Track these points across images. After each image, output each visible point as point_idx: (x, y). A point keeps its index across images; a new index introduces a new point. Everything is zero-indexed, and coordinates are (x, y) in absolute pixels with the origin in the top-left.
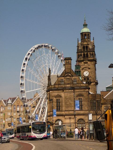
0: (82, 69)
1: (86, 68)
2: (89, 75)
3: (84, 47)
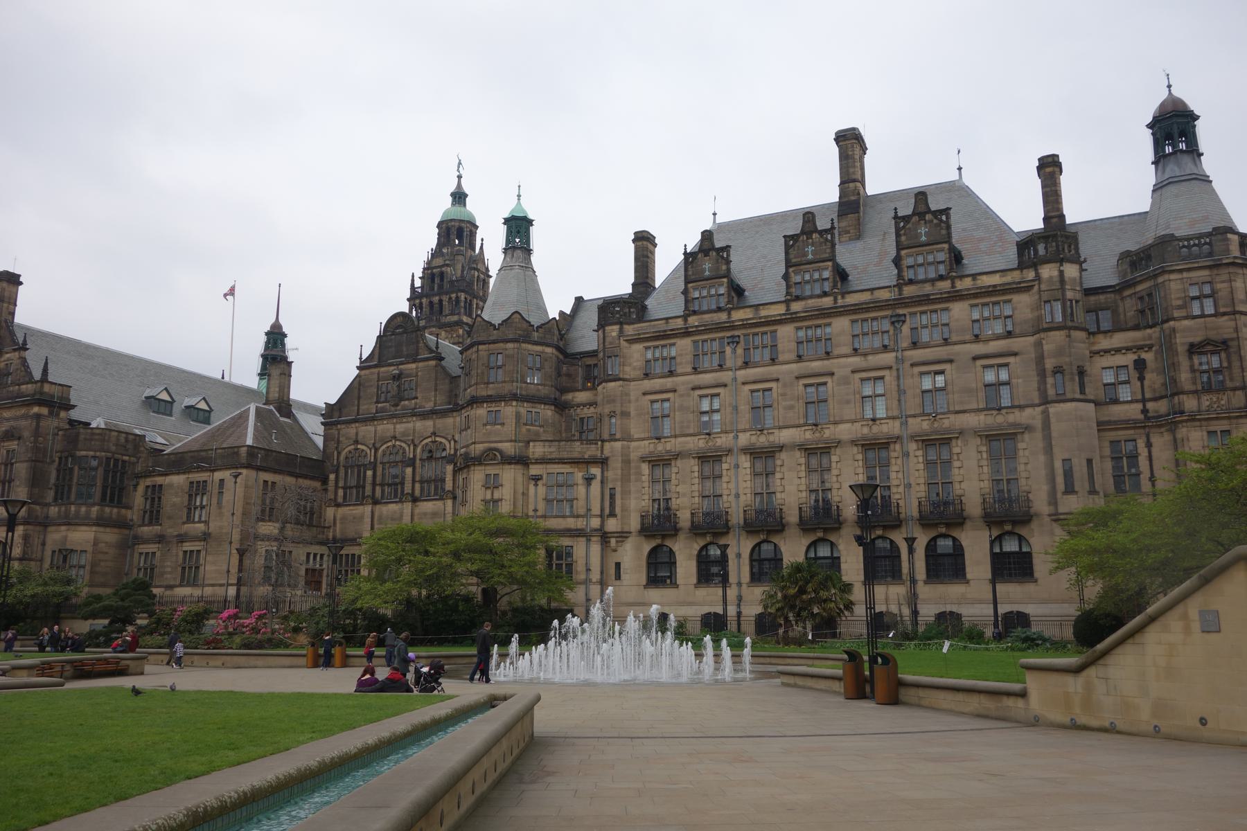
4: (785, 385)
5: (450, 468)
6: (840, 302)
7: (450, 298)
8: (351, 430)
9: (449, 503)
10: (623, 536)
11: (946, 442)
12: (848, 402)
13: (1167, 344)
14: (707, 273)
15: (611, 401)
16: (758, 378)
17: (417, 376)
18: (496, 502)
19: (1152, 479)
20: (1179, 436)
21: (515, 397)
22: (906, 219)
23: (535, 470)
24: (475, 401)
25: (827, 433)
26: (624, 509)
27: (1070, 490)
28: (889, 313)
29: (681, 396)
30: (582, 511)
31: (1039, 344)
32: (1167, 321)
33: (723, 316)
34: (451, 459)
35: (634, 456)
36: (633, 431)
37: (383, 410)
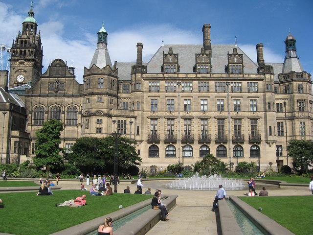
0: (16, 72)
1: (21, 70)
2: (24, 81)
3: (22, 42)
4: (195, 99)
5: (80, 115)
6: (212, 76)
7: (29, 50)
8: (38, 99)
9: (80, 127)
10: (141, 142)
11: (240, 119)
12: (213, 106)
13: (292, 99)
14: (171, 61)
15: (138, 98)
16: (187, 96)
17: (65, 82)
18: (101, 129)
19: (286, 133)
20: (294, 122)
21: (109, 95)
22: (231, 55)
23: (114, 118)
24: (92, 94)
25: (207, 114)
26: (142, 133)
27: (271, 134)
28: (226, 81)
29: (161, 99)
30: (129, 133)
31: (265, 95)
32: (292, 93)
33: (176, 75)
34: (80, 112)
35: (144, 116)
36: (144, 108)
37: (51, 93)
